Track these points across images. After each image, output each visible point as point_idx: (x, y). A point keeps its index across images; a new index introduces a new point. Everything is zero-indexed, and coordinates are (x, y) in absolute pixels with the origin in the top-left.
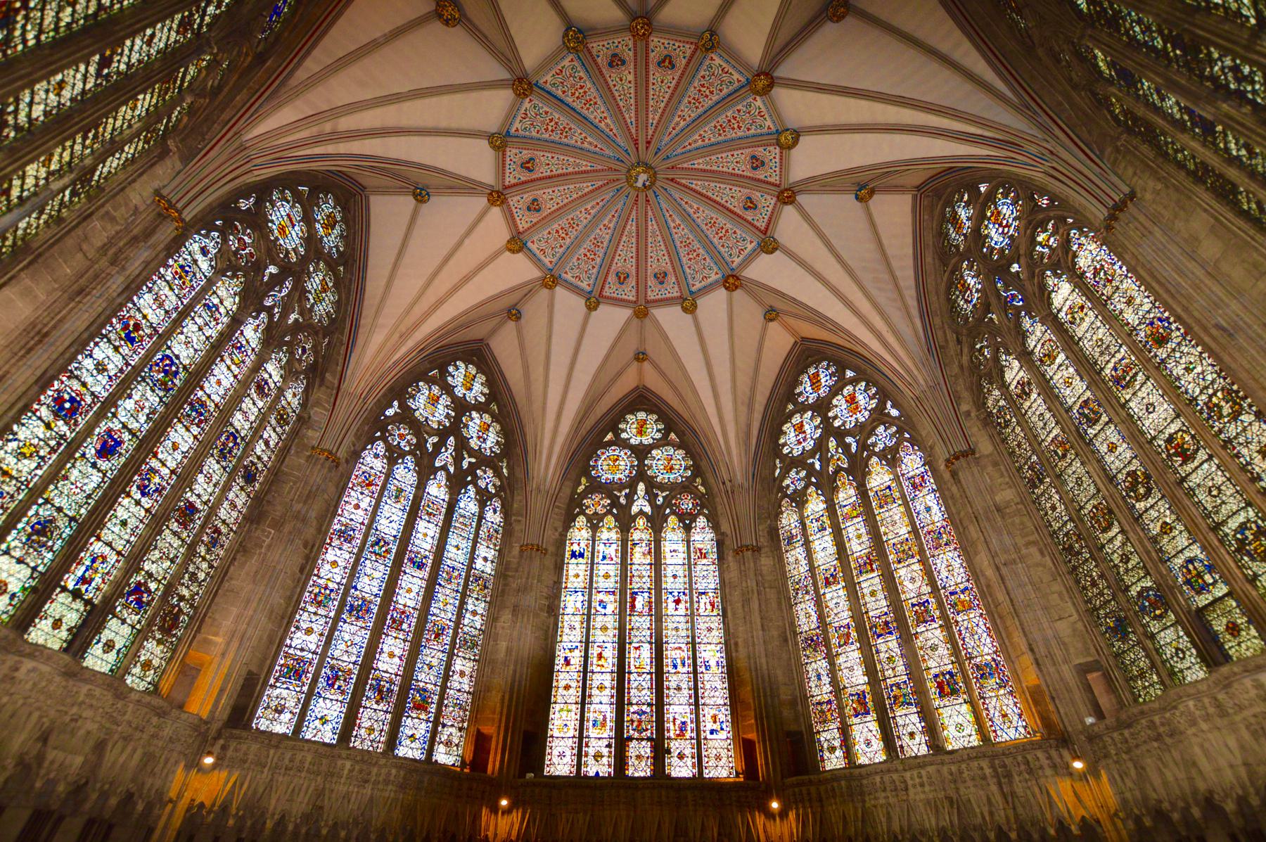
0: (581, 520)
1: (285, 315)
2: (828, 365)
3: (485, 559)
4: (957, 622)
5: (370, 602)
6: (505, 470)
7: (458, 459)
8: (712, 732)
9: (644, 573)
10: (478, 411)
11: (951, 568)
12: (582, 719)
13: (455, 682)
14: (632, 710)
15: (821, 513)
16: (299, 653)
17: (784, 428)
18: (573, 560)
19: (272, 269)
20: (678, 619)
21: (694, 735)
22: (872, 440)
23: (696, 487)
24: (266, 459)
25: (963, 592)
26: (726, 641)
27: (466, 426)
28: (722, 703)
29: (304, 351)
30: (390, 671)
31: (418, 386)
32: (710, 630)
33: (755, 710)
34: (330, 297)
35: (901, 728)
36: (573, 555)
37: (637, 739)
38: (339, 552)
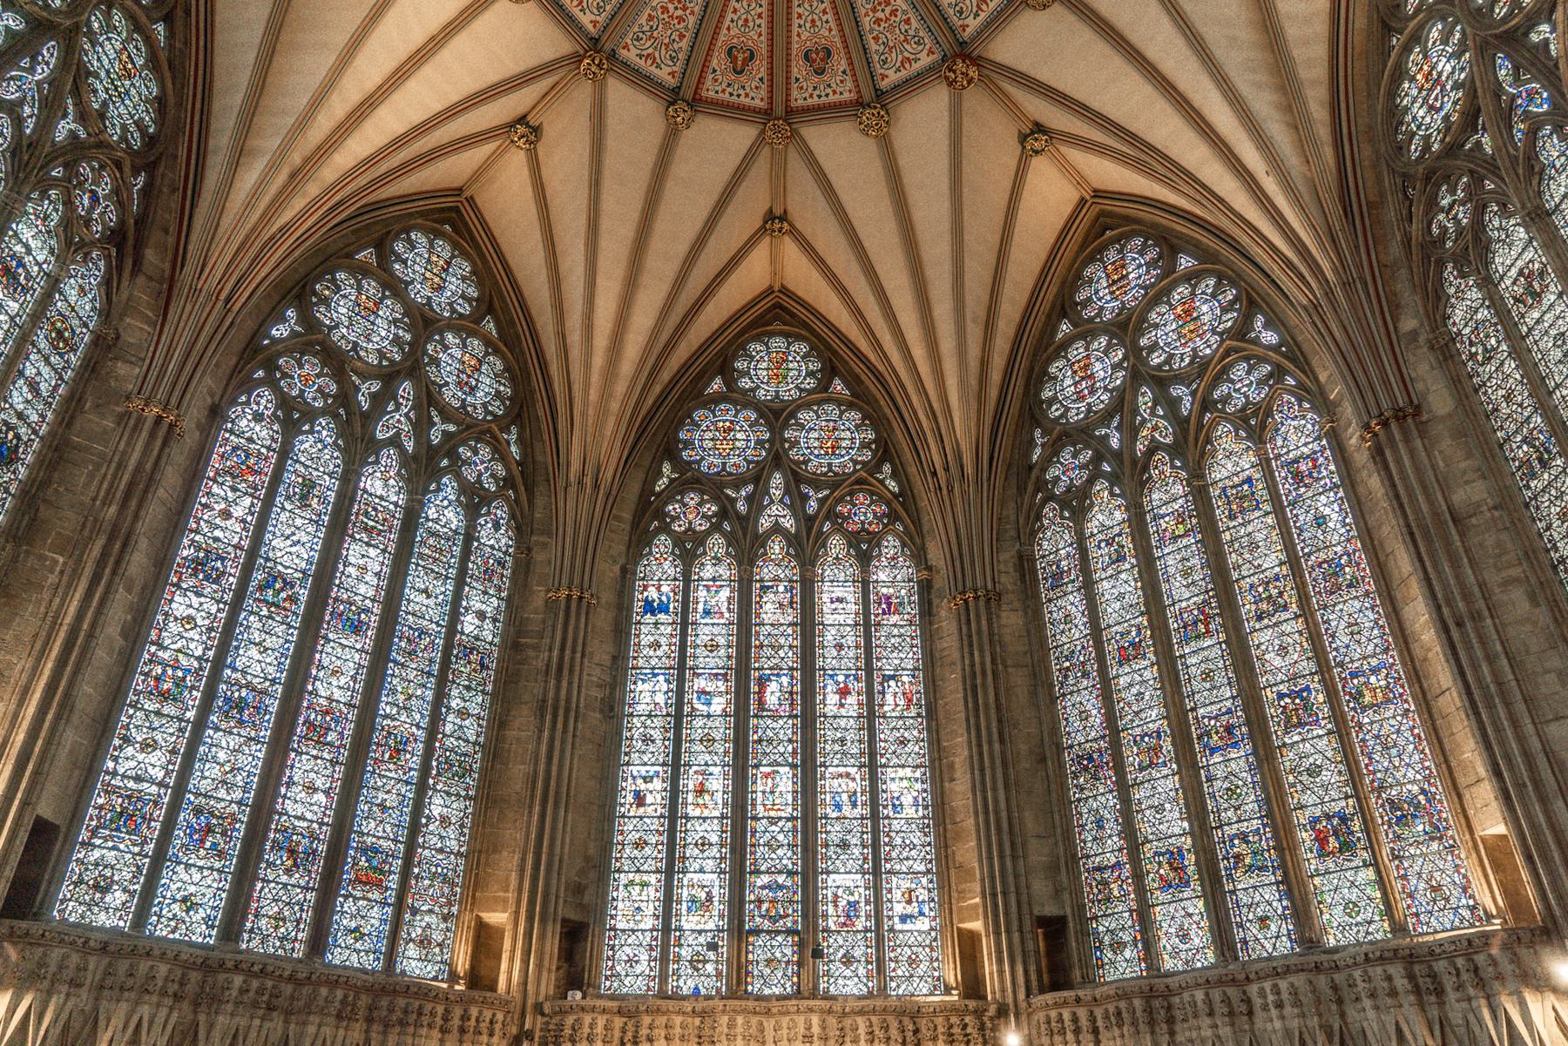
0: (663, 543)
1: (46, 122)
2: (1144, 244)
3: (481, 615)
4: (1360, 725)
5: (264, 692)
6: (513, 449)
7: (421, 426)
8: (904, 918)
9: (782, 641)
10: (457, 330)
11: (1356, 628)
12: (668, 900)
13: (432, 836)
14: (759, 883)
15: (1117, 530)
16: (131, 784)
17: (1052, 370)
18: (649, 618)
20: (843, 723)
21: (871, 924)
22: (1225, 388)
23: (882, 482)
24: (34, 417)
25: (1375, 671)
26: (932, 761)
27: (436, 362)
28: (922, 868)
29: (95, 199)
30: (309, 816)
31: (334, 281)
32: (903, 742)
33: (983, 880)
34: (143, 88)
35: (1245, 910)
36: (649, 607)
37: (768, 932)
38: (195, 601)
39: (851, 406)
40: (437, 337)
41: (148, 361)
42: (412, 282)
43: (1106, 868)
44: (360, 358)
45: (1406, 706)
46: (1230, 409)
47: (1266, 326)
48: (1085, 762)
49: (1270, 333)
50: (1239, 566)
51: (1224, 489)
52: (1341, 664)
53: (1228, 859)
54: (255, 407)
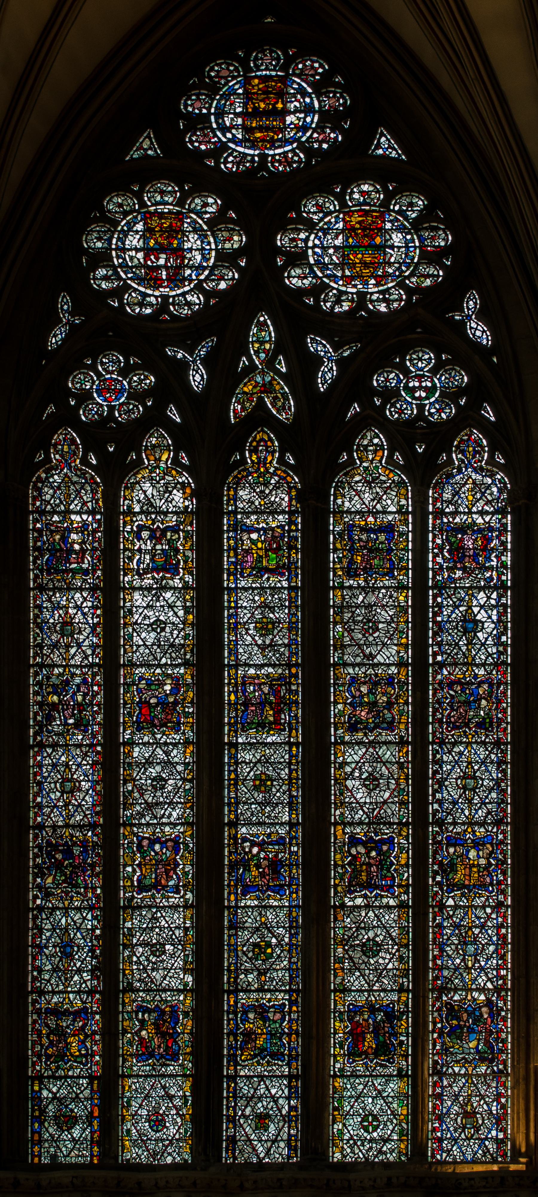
4: (442, 906)
25: (477, 844)
43: (67, 1013)
45: (501, 898)
48: (59, 856)
49: (481, 327)
50: (343, 647)
51: (350, 528)
52: (440, 823)
53: (235, 1036)
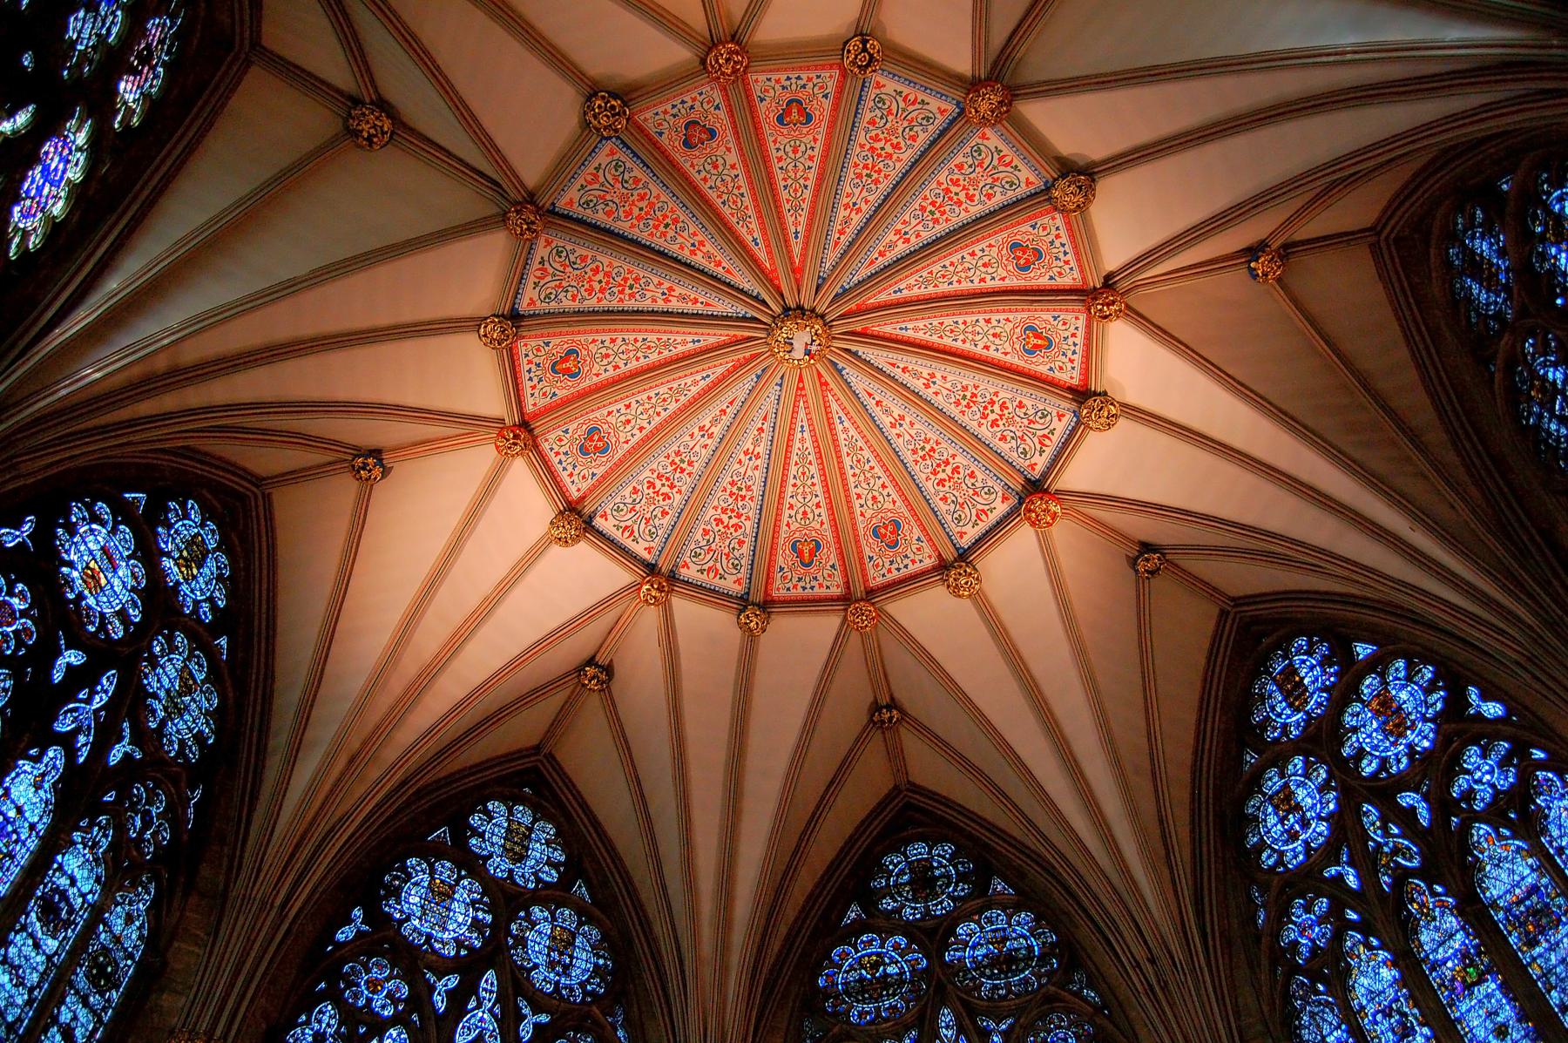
19: (73, 657)
27: (522, 941)
31: (404, 869)
39: (1018, 908)
40: (522, 914)
41: (195, 989)
42: (491, 856)
44: (434, 951)
46: (1478, 806)
47: (1485, 697)
54: (316, 1026)
